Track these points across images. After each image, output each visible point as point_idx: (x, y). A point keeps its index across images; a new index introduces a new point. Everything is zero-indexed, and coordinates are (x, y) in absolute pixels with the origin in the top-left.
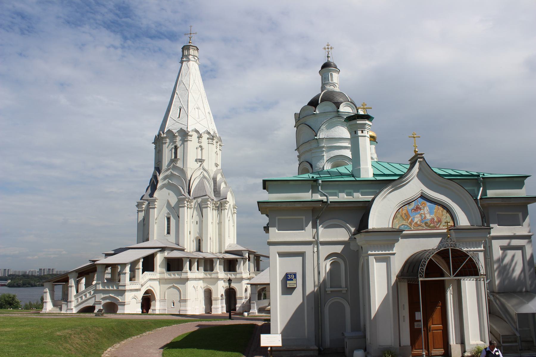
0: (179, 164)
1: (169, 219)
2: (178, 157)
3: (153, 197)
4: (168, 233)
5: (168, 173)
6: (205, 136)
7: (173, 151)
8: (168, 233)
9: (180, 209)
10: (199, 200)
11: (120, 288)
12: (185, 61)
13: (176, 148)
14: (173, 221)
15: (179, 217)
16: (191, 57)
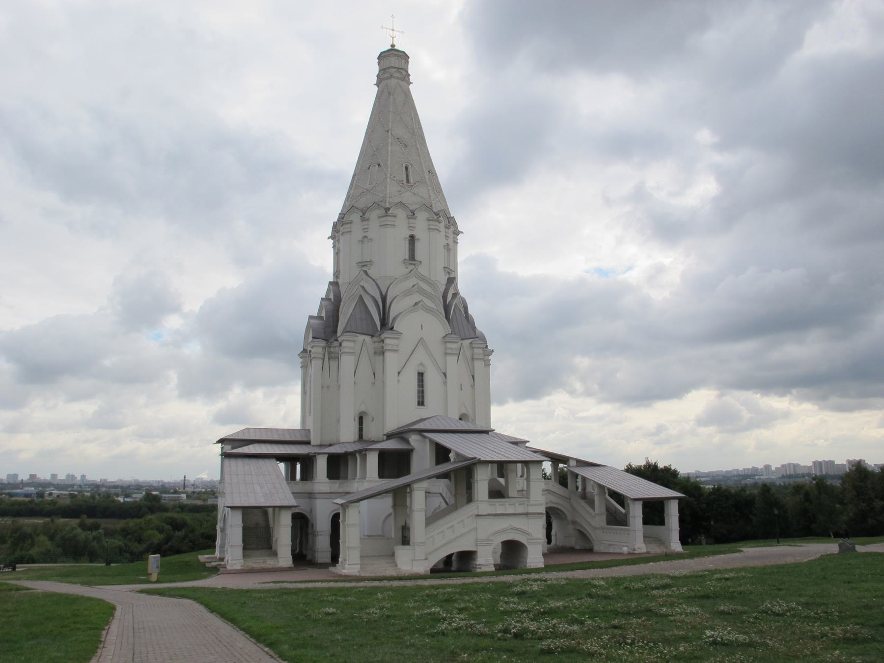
0: (423, 270)
1: (421, 375)
2: (418, 257)
3: (392, 329)
4: (421, 403)
5: (409, 284)
6: (452, 228)
7: (407, 242)
8: (421, 403)
9: (449, 358)
10: (467, 342)
11: (531, 510)
12: (394, 77)
13: (412, 239)
15: (445, 375)
16: (404, 73)
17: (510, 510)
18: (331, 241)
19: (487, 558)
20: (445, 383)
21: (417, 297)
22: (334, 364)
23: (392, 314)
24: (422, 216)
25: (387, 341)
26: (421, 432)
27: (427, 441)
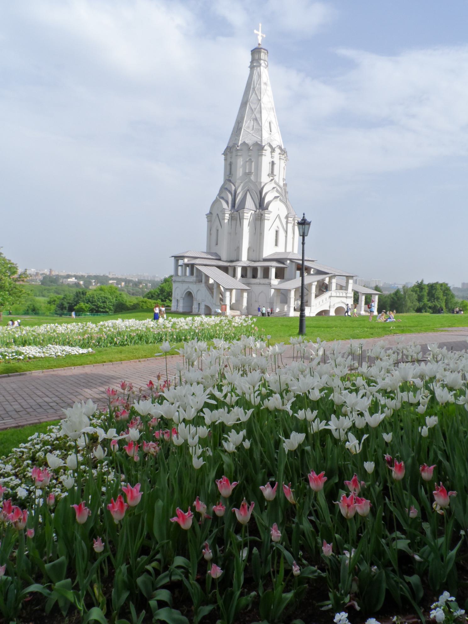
1: (277, 232)
2: (275, 174)
3: (267, 209)
11: (348, 295)
13: (273, 163)
14: (282, 234)
17: (341, 295)
18: (223, 156)
19: (332, 313)
20: (286, 237)
21: (278, 195)
22: (234, 222)
23: (266, 201)
24: (278, 151)
25: (266, 215)
26: (291, 260)
27: (294, 264)
